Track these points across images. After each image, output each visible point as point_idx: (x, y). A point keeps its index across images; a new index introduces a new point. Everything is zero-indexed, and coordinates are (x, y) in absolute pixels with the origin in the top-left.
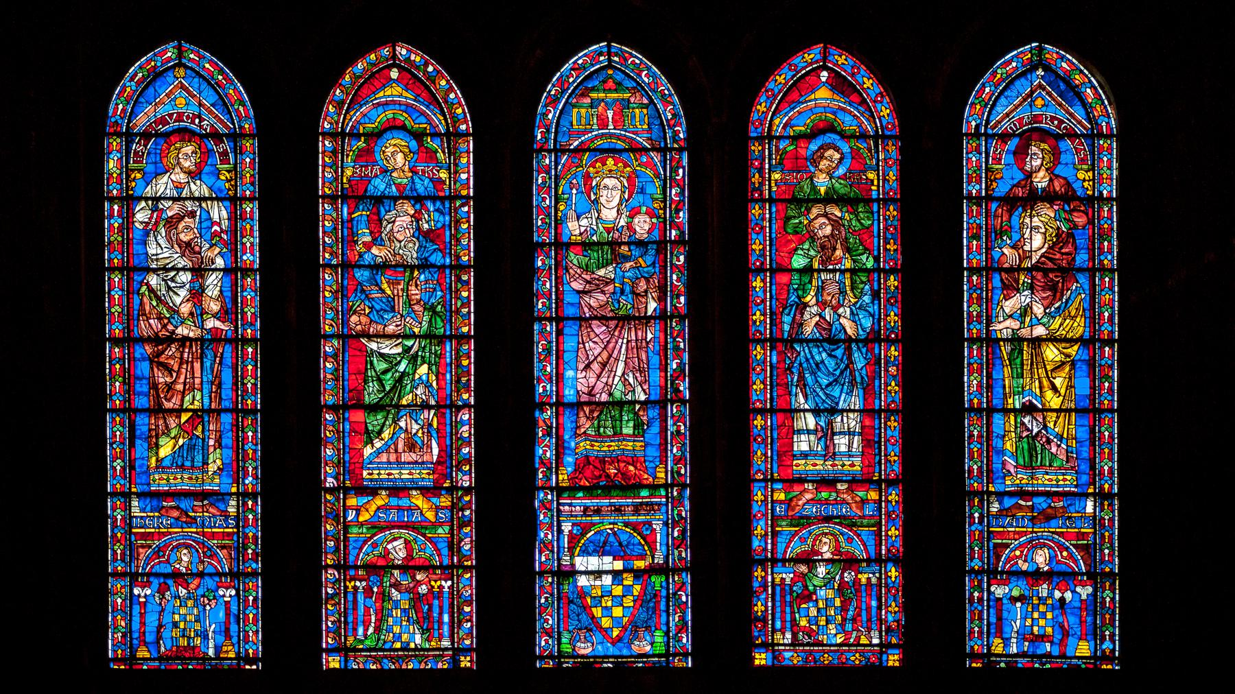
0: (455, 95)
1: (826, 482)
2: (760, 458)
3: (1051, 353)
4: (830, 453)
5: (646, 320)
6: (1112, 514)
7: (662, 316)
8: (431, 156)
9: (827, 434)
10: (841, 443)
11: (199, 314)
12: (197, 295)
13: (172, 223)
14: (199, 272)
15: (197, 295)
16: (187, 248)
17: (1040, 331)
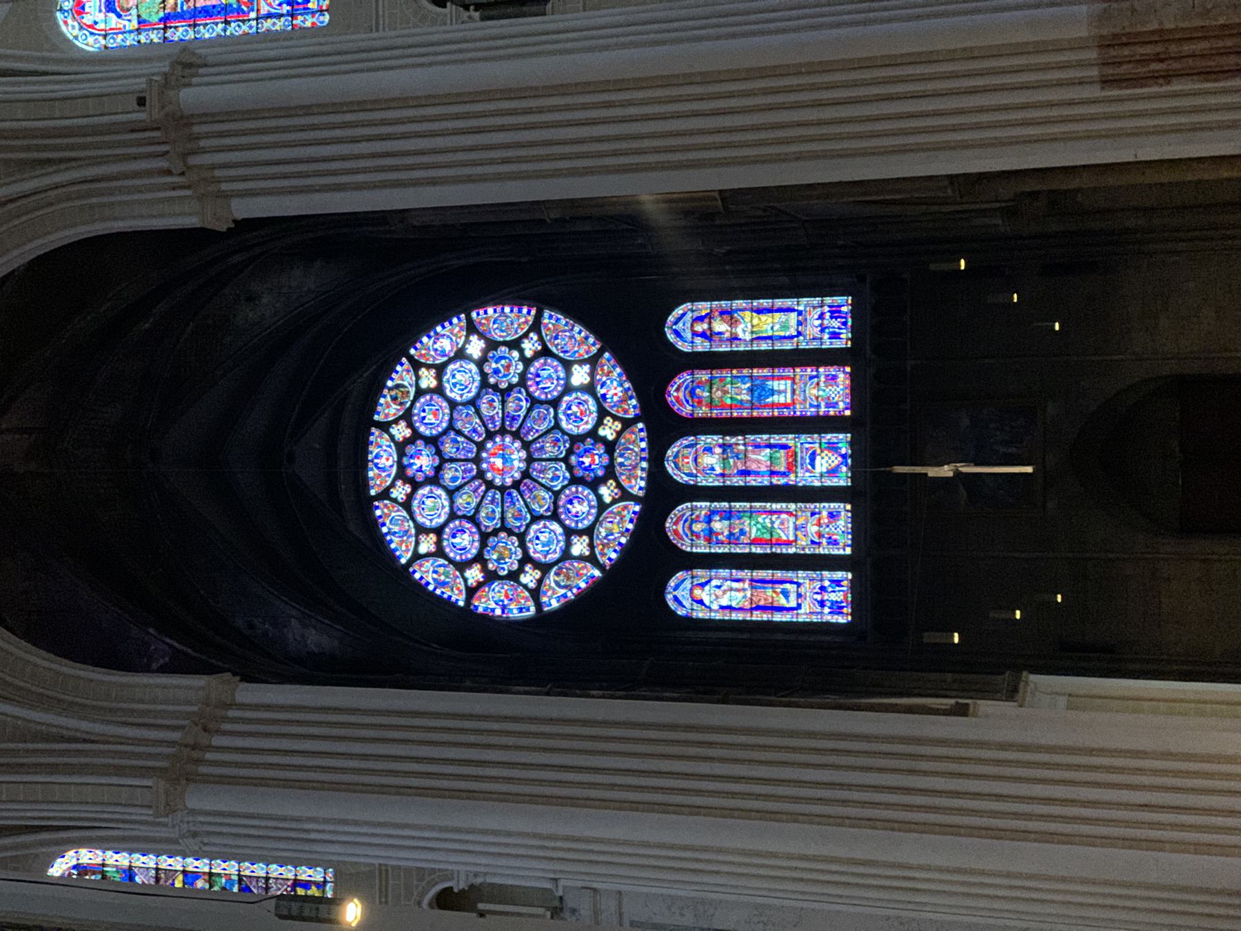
0: (679, 508)
1: (794, 392)
2: (786, 412)
3: (755, 321)
4: (785, 391)
5: (746, 450)
6: (804, 300)
7: (745, 445)
8: (698, 517)
9: (780, 392)
10: (782, 387)
11: (744, 590)
12: (738, 590)
13: (717, 597)
14: (731, 589)
15: (738, 590)
16: (724, 592)
17: (749, 325)
